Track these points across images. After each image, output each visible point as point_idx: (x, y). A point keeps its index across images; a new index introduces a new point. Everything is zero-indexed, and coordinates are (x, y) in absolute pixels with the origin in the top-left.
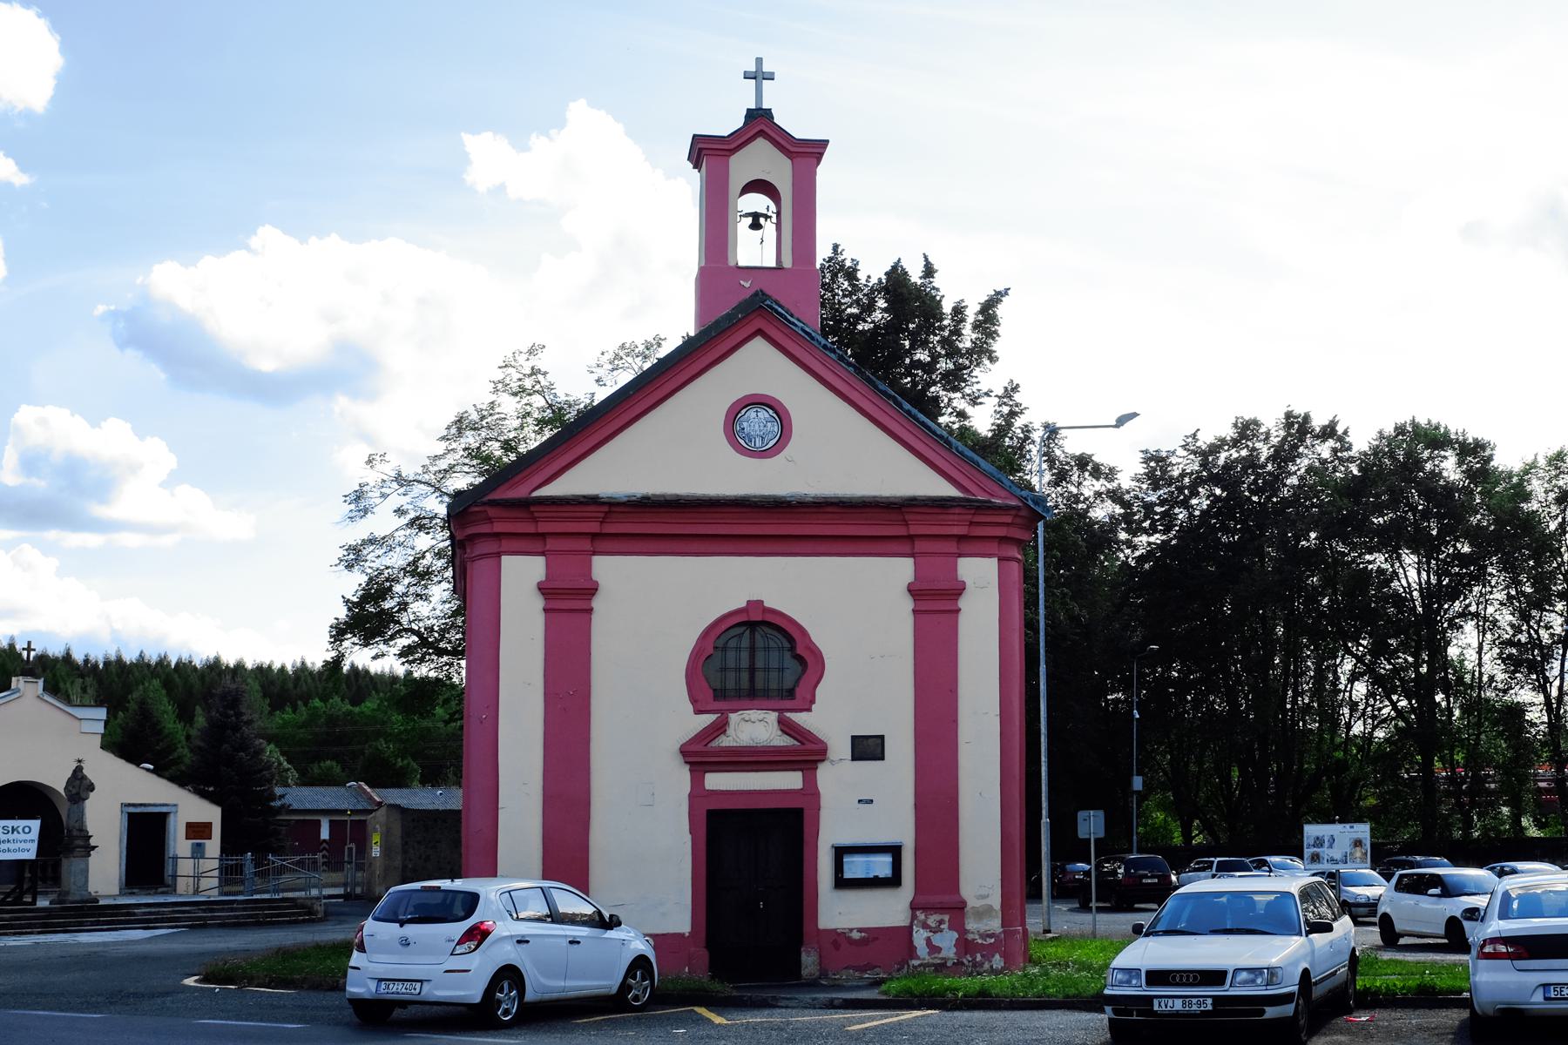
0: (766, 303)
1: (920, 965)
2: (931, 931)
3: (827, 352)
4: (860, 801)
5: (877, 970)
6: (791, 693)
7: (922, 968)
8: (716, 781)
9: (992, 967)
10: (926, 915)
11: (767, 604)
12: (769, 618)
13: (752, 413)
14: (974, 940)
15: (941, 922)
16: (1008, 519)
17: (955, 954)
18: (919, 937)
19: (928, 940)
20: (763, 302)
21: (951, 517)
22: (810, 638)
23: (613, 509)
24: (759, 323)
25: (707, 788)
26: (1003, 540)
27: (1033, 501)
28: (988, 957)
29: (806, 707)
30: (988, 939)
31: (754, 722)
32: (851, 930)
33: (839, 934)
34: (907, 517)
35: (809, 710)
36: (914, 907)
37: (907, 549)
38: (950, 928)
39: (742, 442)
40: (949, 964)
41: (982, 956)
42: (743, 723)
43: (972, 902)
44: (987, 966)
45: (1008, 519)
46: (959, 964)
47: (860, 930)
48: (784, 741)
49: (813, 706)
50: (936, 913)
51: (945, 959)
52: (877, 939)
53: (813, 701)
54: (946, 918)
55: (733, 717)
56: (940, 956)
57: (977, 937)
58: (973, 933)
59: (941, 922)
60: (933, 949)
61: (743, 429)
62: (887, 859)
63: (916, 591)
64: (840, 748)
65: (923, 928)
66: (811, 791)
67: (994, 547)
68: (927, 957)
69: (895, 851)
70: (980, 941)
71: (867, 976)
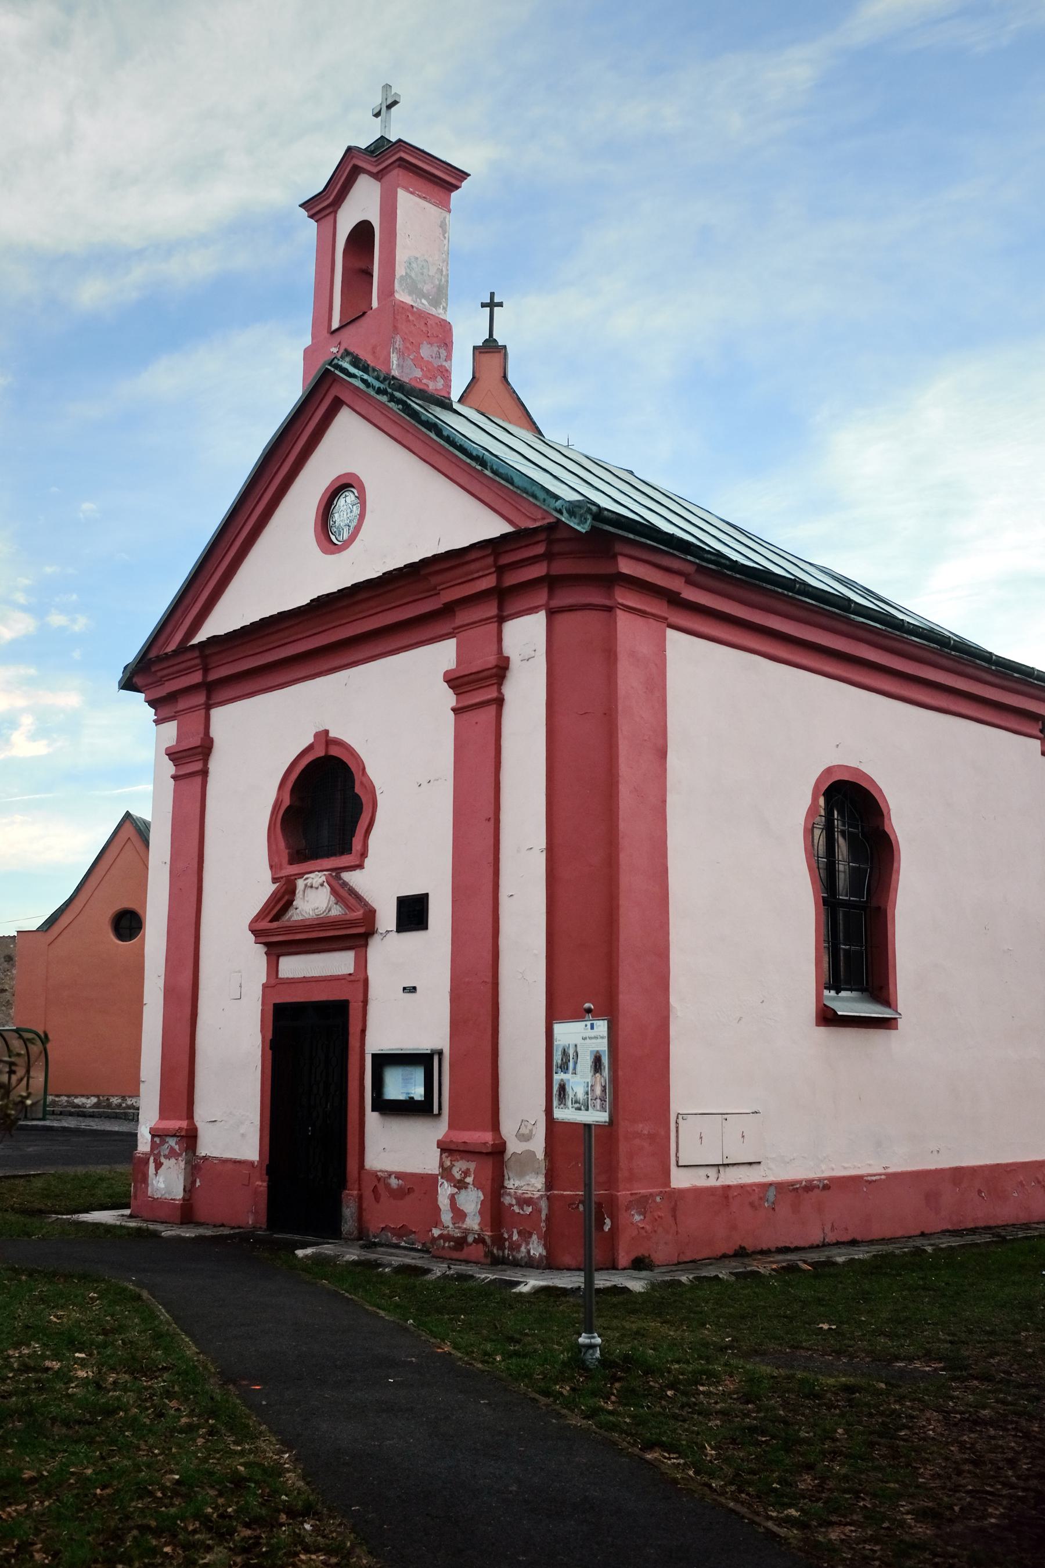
0: (333, 363)
1: (441, 1236)
2: (455, 1186)
3: (379, 397)
4: (404, 989)
5: (412, 1236)
6: (345, 848)
7: (442, 1241)
8: (293, 966)
9: (529, 1252)
10: (451, 1161)
11: (332, 734)
12: (334, 751)
13: (342, 501)
14: (511, 1205)
15: (466, 1173)
16: (540, 549)
17: (479, 1224)
18: (445, 1190)
19: (452, 1198)
20: (330, 364)
21: (473, 566)
22: (364, 769)
23: (208, 652)
24: (334, 392)
25: (281, 975)
26: (552, 583)
27: (568, 511)
28: (526, 1235)
29: (357, 863)
30: (525, 1208)
31: (317, 888)
32: (390, 1174)
33: (379, 1179)
34: (434, 580)
35: (360, 866)
36: (446, 1148)
37: (447, 628)
38: (478, 1185)
39: (333, 538)
40: (470, 1239)
41: (519, 1233)
42: (309, 891)
43: (514, 1147)
44: (523, 1249)
45: (540, 549)
46: (480, 1240)
47: (399, 1176)
48: (337, 911)
49: (366, 860)
50: (462, 1159)
51: (467, 1232)
52: (410, 1190)
53: (364, 854)
54: (472, 1166)
55: (300, 883)
56: (465, 1226)
57: (514, 1202)
58: (509, 1194)
59: (466, 1173)
60: (459, 1215)
61: (335, 522)
62: (418, 1074)
63: (455, 682)
64: (387, 917)
65: (447, 1181)
66: (360, 980)
67: (542, 597)
68: (451, 1226)
69: (424, 1060)
70: (516, 1209)
71: (403, 1244)
